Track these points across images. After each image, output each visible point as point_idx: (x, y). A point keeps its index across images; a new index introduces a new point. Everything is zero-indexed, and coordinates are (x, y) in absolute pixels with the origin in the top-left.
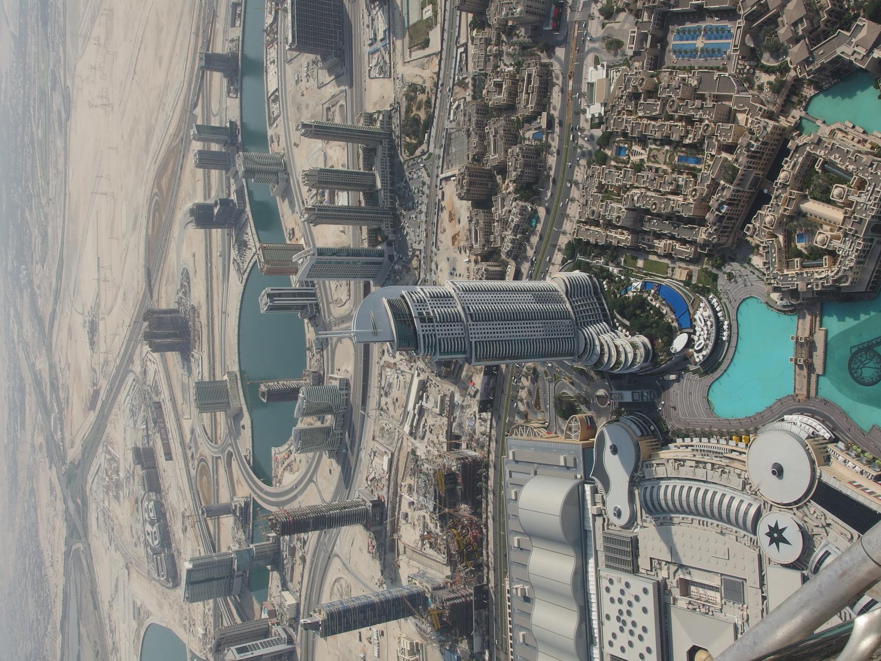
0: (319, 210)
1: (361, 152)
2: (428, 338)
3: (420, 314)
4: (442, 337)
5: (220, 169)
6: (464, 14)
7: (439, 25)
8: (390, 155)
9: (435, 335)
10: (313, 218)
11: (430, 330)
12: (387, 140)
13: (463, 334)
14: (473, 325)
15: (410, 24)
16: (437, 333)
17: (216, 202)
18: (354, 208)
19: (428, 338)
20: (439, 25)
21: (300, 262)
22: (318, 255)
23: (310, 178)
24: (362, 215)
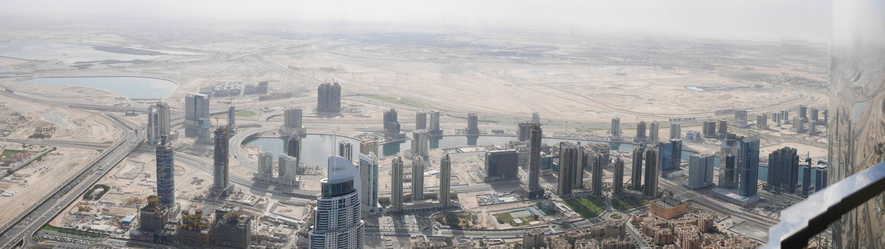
0: (400, 165)
1: (435, 192)
2: (329, 204)
3: (345, 199)
4: (332, 204)
5: (417, 126)
6: (522, 239)
7: (512, 227)
8: (434, 208)
9: (330, 209)
10: (395, 162)
11: (334, 204)
12: (443, 206)
13: (330, 228)
14: (336, 236)
15: (510, 214)
16: (332, 211)
17: (398, 123)
18: (402, 191)
19: (329, 204)
20: (512, 227)
21: (370, 155)
22: (374, 166)
23: (418, 162)
24: (398, 196)
